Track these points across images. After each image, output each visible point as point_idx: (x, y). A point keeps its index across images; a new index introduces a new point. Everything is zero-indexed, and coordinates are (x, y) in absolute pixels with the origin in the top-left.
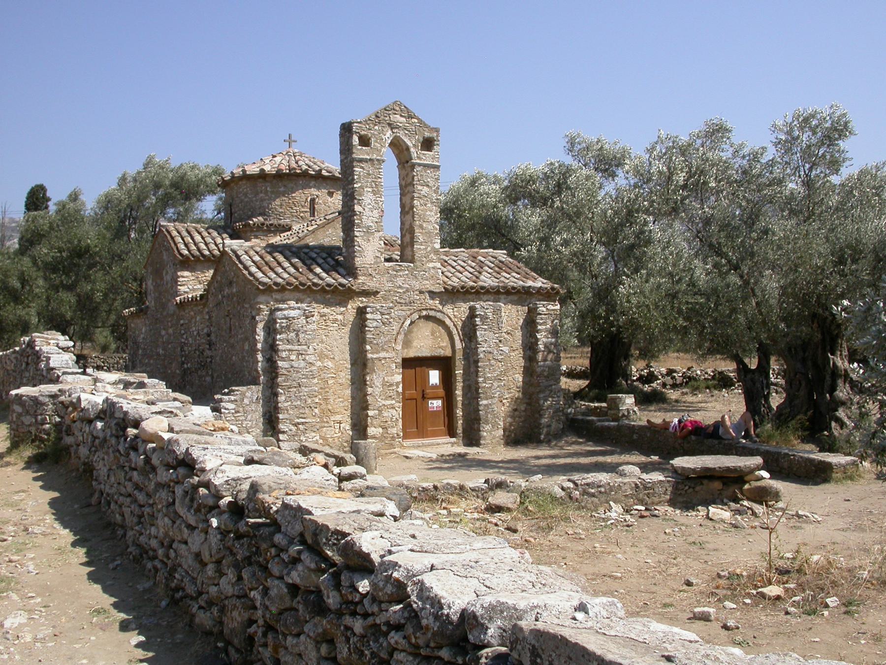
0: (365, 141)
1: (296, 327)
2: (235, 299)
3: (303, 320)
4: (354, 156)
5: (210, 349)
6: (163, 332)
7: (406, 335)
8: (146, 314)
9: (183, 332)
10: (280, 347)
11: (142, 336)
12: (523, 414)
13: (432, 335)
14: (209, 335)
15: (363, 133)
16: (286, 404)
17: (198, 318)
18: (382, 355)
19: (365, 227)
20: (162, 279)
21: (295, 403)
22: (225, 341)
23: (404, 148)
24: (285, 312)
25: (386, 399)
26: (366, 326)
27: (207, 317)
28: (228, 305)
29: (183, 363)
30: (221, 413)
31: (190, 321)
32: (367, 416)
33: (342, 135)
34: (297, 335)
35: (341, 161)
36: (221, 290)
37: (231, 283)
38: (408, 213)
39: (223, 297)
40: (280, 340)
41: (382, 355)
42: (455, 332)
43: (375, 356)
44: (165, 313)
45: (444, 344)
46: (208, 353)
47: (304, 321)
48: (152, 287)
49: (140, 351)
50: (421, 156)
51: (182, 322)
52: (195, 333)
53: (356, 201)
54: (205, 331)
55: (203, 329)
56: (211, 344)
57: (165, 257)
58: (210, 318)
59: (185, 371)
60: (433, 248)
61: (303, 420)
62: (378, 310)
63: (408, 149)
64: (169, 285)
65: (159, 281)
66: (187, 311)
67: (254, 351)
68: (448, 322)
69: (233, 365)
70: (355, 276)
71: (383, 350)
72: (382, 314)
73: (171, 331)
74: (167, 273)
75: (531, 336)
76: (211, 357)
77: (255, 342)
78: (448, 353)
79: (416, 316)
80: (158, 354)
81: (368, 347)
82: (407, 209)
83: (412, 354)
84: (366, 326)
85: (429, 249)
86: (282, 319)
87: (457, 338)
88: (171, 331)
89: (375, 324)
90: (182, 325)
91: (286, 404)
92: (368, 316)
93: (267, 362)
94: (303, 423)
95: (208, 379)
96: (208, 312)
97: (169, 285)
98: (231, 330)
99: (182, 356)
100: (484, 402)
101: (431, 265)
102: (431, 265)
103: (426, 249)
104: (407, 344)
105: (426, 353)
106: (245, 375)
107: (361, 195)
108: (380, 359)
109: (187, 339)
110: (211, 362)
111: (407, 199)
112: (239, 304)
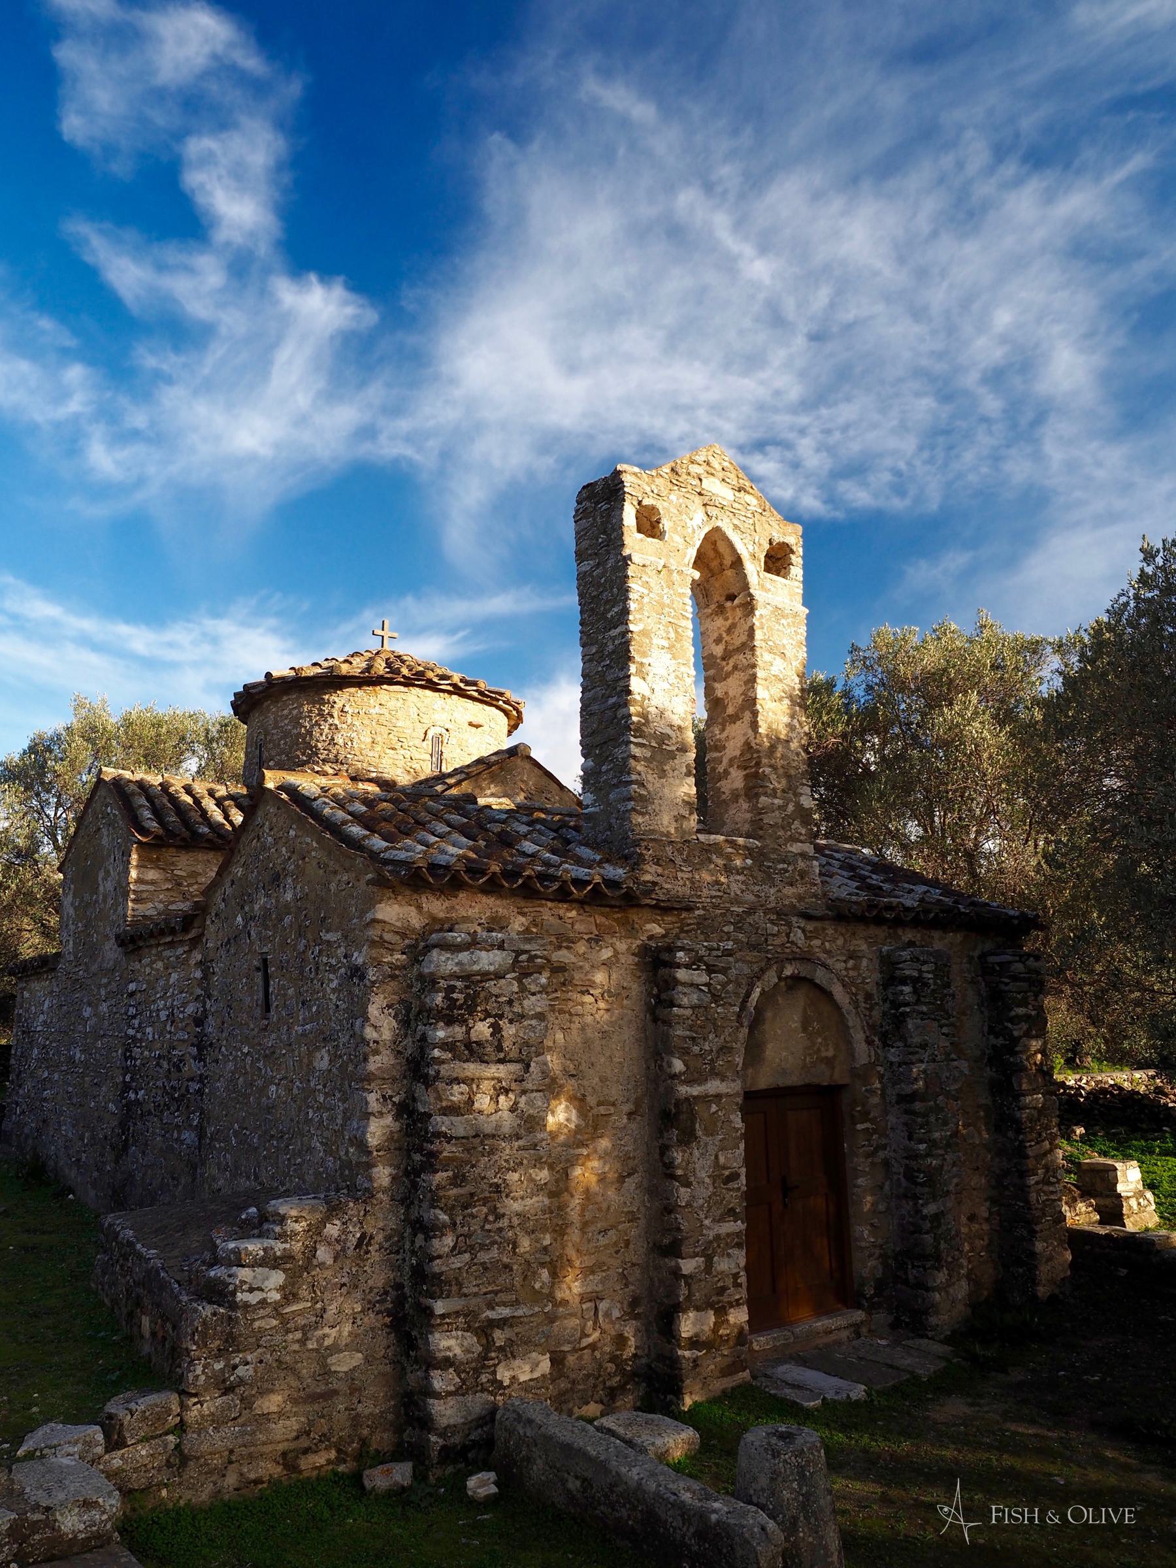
0: (650, 524)
1: (491, 1006)
2: (288, 919)
3: (508, 985)
4: (626, 552)
5: (199, 1058)
6: (87, 1012)
7: (752, 1028)
8: (54, 969)
9: (132, 1011)
10: (444, 1070)
11: (42, 1018)
12: (986, 1227)
13: (805, 1030)
14: (199, 1021)
15: (646, 502)
16: (457, 1262)
17: (174, 976)
18: (714, 1086)
19: (654, 736)
20: (95, 891)
21: (483, 1257)
22: (246, 1040)
23: (728, 561)
24: (464, 956)
25: (721, 1220)
26: (672, 1004)
27: (198, 974)
28: (263, 940)
29: (126, 1087)
30: (233, 1306)
31: (152, 985)
32: (676, 1273)
33: (581, 515)
34: (496, 1029)
35: (581, 577)
36: (244, 900)
37: (276, 879)
38: (734, 718)
39: (249, 919)
40: (445, 1046)
41: (714, 1086)
42: (852, 1020)
43: (695, 1091)
44: (94, 968)
45: (830, 1053)
46: (192, 1067)
47: (515, 988)
48: (71, 911)
49: (36, 1051)
50: (768, 586)
51: (132, 987)
52: (163, 1015)
53: (633, 668)
54: (190, 1009)
55: (184, 1005)
56: (202, 1045)
57: (105, 841)
58: (206, 976)
59: (129, 1105)
60: (799, 806)
61: (505, 1312)
62: (700, 959)
63: (738, 562)
64: (109, 905)
65: (87, 897)
66: (146, 961)
67: (350, 1076)
68: (838, 991)
69: (269, 1109)
70: (634, 862)
71: (715, 1074)
72: (710, 970)
73: (104, 1008)
74: (107, 873)
75: (991, 1031)
76: (201, 1079)
77: (361, 1049)
78: (839, 1076)
79: (771, 977)
80: (71, 1060)
81: (678, 1065)
82: (730, 710)
83: (763, 1082)
84: (672, 1004)
85: (791, 808)
86: (458, 978)
87: (859, 1036)
88: (104, 1008)
89: (694, 998)
90: (132, 995)
91: (457, 1262)
92: (681, 974)
93: (397, 1117)
94: (502, 1323)
95: (189, 1136)
96: (200, 964)
97: (109, 905)
98: (267, 1007)
99: (126, 1070)
100: (931, 1209)
101: (795, 848)
102: (795, 848)
103: (782, 808)
104: (754, 1050)
105: (794, 1080)
106: (310, 1150)
107: (644, 654)
108: (705, 1099)
109: (140, 1029)
110: (200, 1092)
111: (731, 688)
112: (301, 934)
